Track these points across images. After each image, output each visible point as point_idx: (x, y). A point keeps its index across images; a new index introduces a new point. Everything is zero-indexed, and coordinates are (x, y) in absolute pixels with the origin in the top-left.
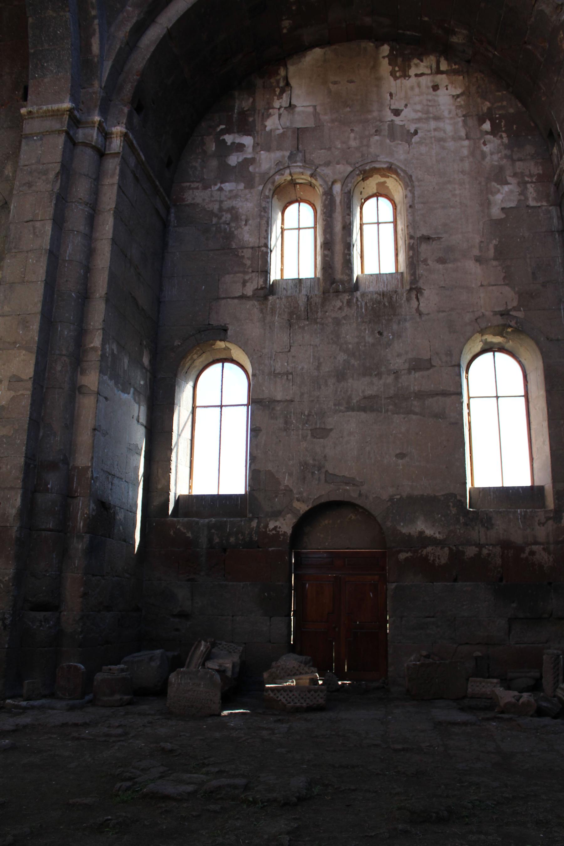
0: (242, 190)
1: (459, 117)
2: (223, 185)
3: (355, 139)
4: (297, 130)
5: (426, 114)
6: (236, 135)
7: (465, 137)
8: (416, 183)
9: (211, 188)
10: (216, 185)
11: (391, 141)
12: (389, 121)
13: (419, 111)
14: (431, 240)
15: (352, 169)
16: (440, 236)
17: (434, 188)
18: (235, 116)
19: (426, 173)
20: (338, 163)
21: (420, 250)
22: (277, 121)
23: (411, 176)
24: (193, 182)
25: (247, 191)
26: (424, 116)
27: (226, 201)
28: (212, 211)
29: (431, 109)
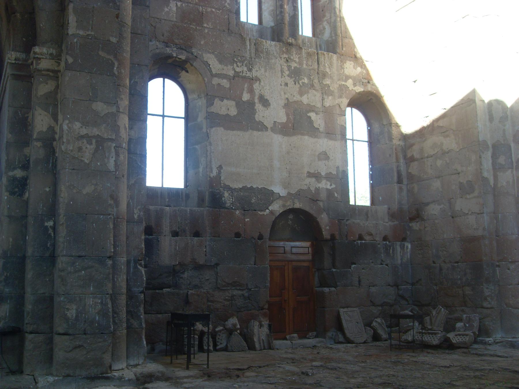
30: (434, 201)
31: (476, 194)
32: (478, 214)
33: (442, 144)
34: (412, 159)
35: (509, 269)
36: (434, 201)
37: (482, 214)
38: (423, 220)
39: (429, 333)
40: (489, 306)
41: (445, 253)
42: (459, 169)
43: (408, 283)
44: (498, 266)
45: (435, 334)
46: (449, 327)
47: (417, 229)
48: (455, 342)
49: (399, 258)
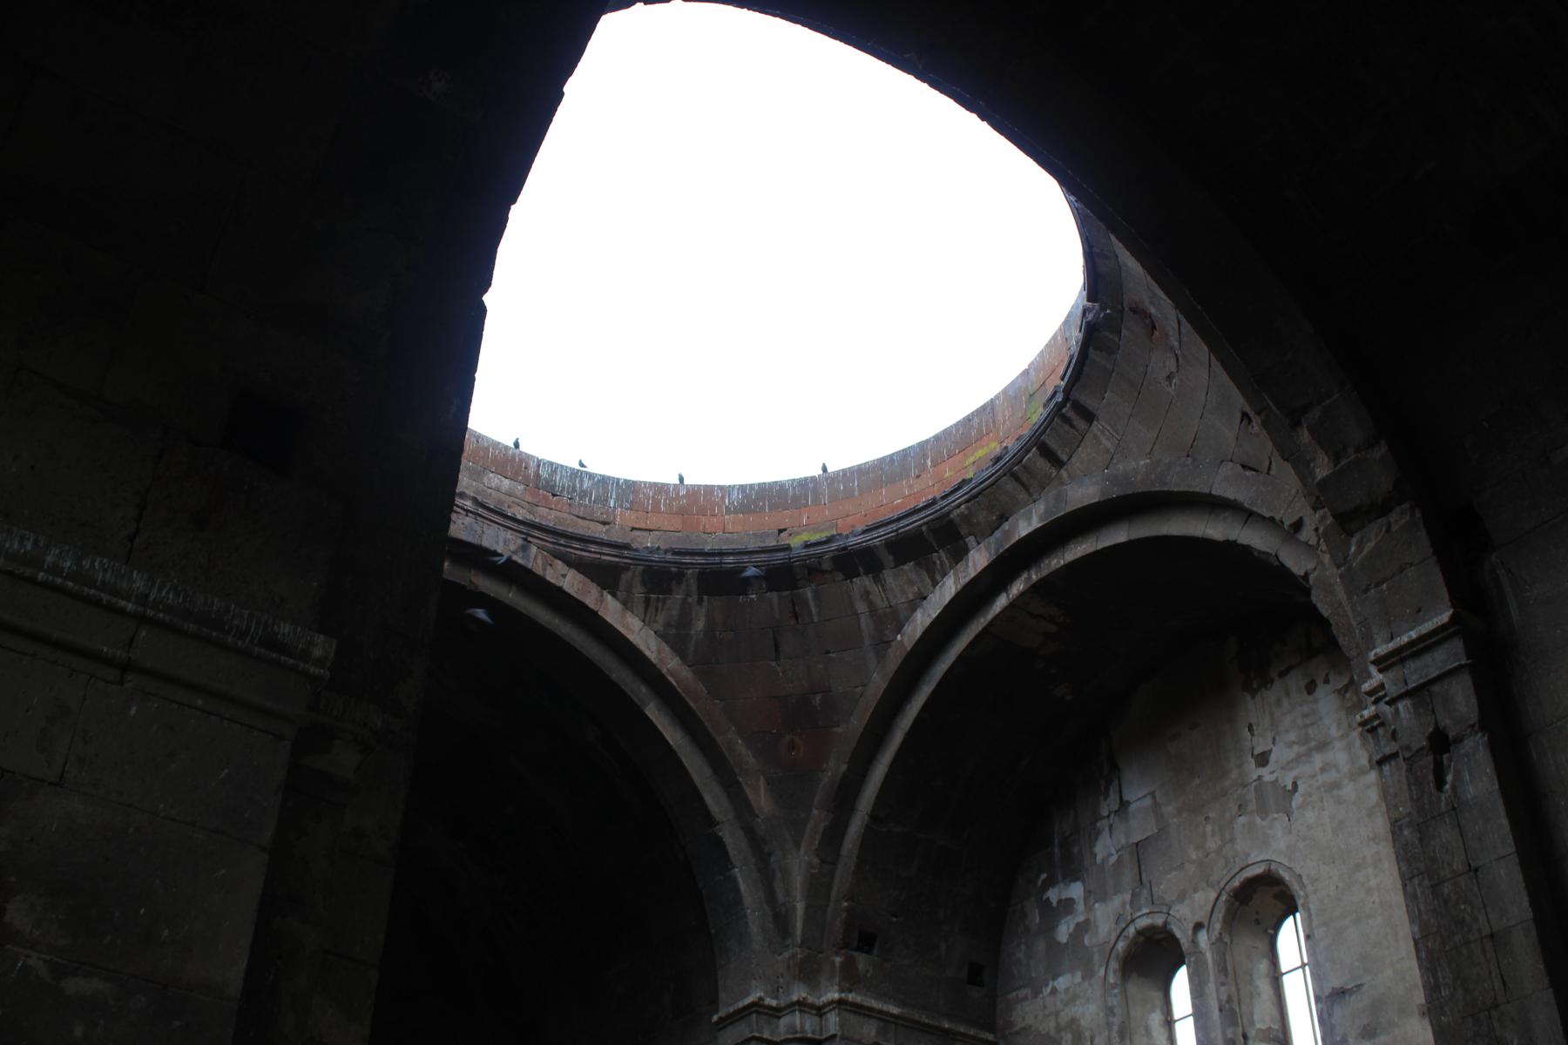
0: (1079, 984)
1: (1354, 729)
2: (1055, 983)
3: (1213, 835)
4: (1135, 846)
5: (1304, 744)
6: (1062, 885)
7: (1368, 766)
8: (1310, 888)
9: (1042, 992)
10: (1047, 985)
11: (1263, 819)
12: (1255, 781)
13: (1294, 743)
14: (1347, 997)
15: (1216, 895)
16: (1359, 983)
17: (1337, 887)
18: (1056, 850)
19: (1321, 863)
20: (1196, 891)
21: (1333, 1021)
22: (1109, 841)
23: (1300, 876)
24: (1017, 989)
25: (1086, 984)
26: (1303, 749)
27: (1063, 1011)
28: (1048, 1033)
29: (1310, 730)
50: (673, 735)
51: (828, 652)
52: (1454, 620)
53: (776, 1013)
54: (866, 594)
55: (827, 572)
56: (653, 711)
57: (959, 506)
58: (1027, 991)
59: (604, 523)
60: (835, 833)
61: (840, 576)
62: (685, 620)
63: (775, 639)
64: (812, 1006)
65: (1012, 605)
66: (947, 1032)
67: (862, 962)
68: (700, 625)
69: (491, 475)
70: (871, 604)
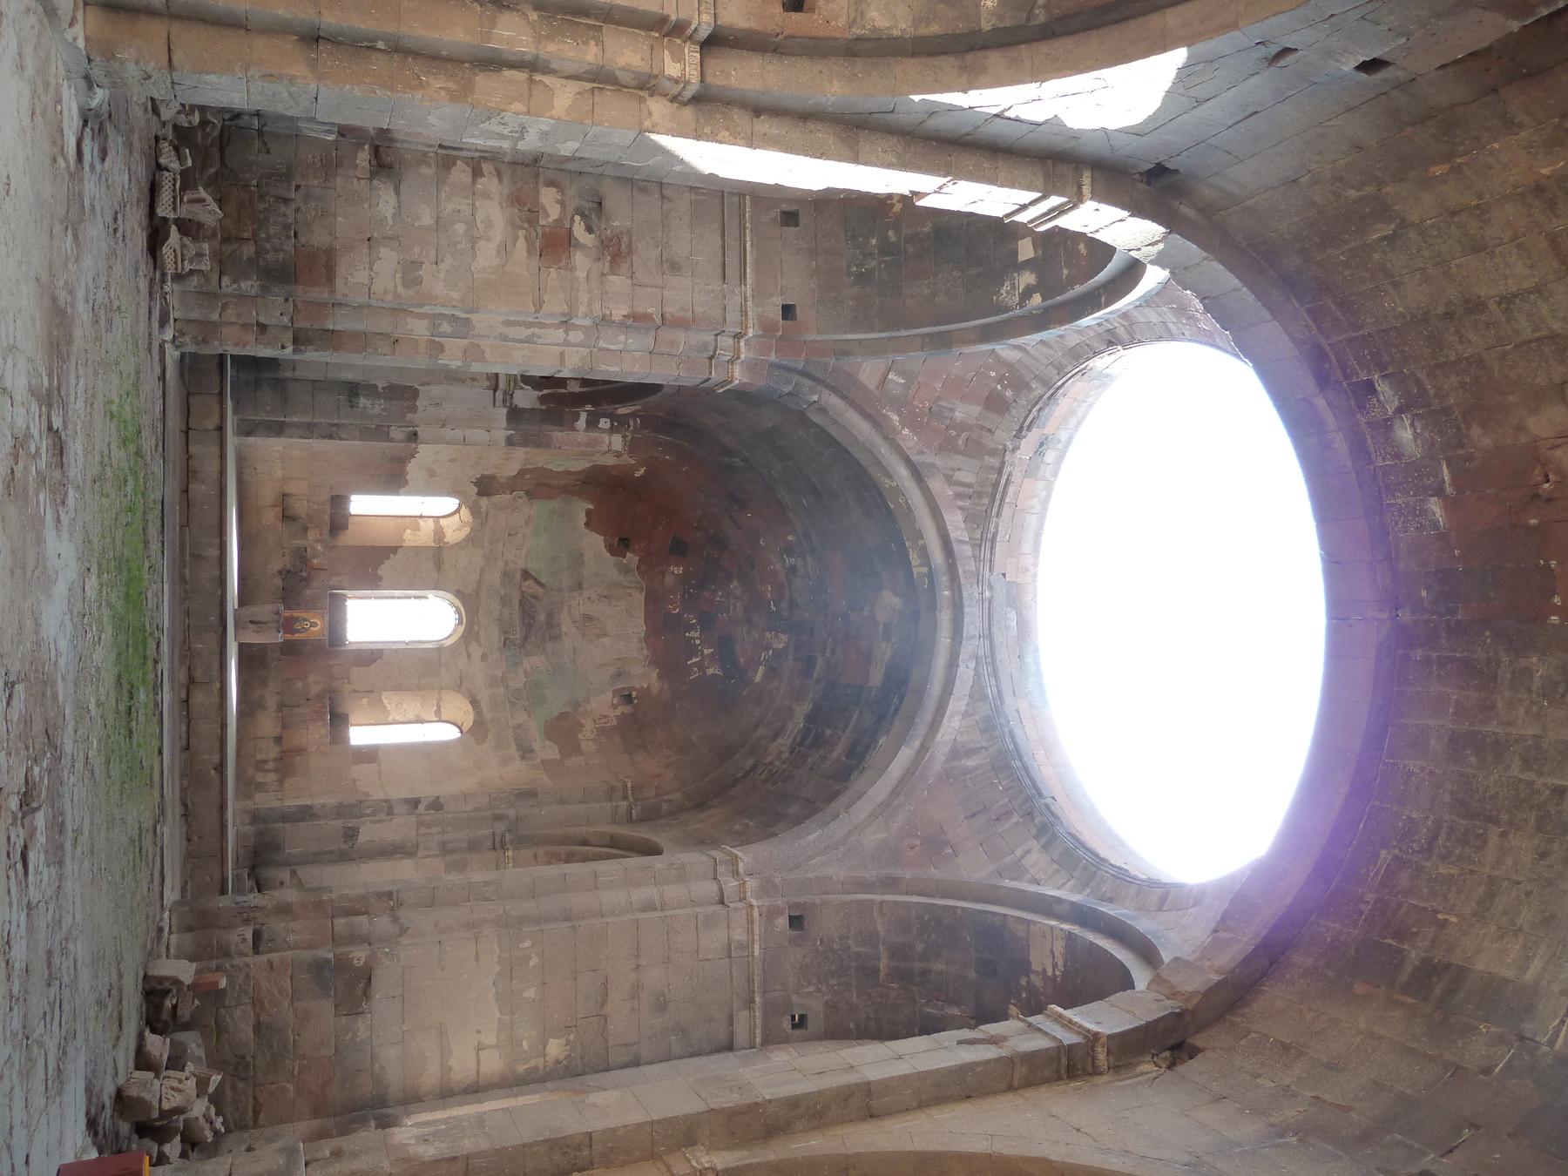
24: (795, 1050)
30: (399, 207)
31: (400, 290)
32: (369, 289)
33: (488, 240)
34: (477, 173)
35: (281, 314)
36: (399, 207)
37: (369, 296)
38: (371, 179)
39: (174, 198)
40: (223, 284)
41: (313, 214)
42: (444, 266)
43: (262, 126)
44: (287, 300)
45: (174, 209)
46: (188, 228)
47: (358, 162)
48: (164, 252)
49: (310, 126)
50: (896, 769)
51: (981, 845)
52: (1096, 1036)
53: (736, 873)
54: (1029, 851)
55: (1033, 820)
56: (905, 755)
57: (1106, 872)
58: (796, 1054)
59: (1014, 693)
60: (865, 886)
61: (1034, 831)
62: (971, 752)
63: (979, 812)
64: (745, 893)
65: (1052, 928)
66: (753, 1001)
67: (782, 922)
68: (970, 763)
69: (1014, 613)
70: (1023, 857)
